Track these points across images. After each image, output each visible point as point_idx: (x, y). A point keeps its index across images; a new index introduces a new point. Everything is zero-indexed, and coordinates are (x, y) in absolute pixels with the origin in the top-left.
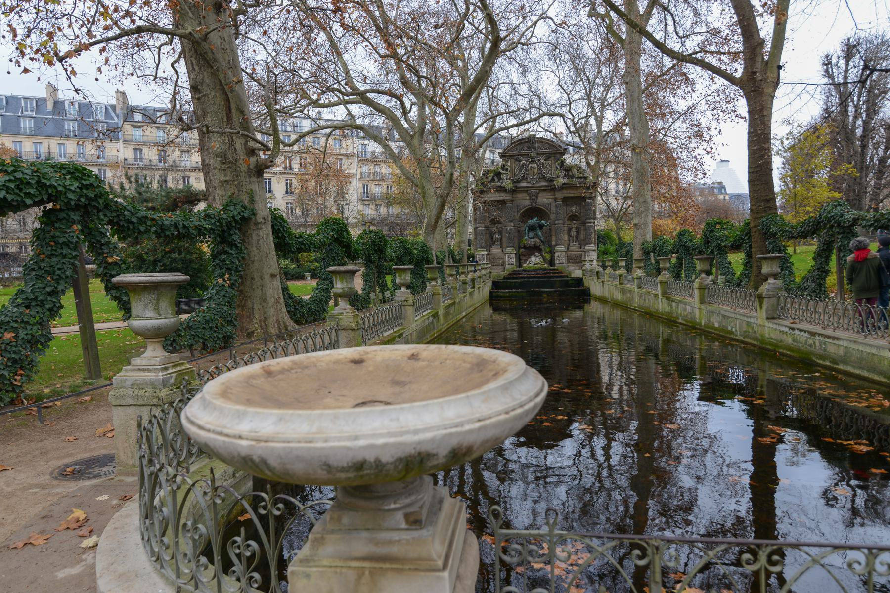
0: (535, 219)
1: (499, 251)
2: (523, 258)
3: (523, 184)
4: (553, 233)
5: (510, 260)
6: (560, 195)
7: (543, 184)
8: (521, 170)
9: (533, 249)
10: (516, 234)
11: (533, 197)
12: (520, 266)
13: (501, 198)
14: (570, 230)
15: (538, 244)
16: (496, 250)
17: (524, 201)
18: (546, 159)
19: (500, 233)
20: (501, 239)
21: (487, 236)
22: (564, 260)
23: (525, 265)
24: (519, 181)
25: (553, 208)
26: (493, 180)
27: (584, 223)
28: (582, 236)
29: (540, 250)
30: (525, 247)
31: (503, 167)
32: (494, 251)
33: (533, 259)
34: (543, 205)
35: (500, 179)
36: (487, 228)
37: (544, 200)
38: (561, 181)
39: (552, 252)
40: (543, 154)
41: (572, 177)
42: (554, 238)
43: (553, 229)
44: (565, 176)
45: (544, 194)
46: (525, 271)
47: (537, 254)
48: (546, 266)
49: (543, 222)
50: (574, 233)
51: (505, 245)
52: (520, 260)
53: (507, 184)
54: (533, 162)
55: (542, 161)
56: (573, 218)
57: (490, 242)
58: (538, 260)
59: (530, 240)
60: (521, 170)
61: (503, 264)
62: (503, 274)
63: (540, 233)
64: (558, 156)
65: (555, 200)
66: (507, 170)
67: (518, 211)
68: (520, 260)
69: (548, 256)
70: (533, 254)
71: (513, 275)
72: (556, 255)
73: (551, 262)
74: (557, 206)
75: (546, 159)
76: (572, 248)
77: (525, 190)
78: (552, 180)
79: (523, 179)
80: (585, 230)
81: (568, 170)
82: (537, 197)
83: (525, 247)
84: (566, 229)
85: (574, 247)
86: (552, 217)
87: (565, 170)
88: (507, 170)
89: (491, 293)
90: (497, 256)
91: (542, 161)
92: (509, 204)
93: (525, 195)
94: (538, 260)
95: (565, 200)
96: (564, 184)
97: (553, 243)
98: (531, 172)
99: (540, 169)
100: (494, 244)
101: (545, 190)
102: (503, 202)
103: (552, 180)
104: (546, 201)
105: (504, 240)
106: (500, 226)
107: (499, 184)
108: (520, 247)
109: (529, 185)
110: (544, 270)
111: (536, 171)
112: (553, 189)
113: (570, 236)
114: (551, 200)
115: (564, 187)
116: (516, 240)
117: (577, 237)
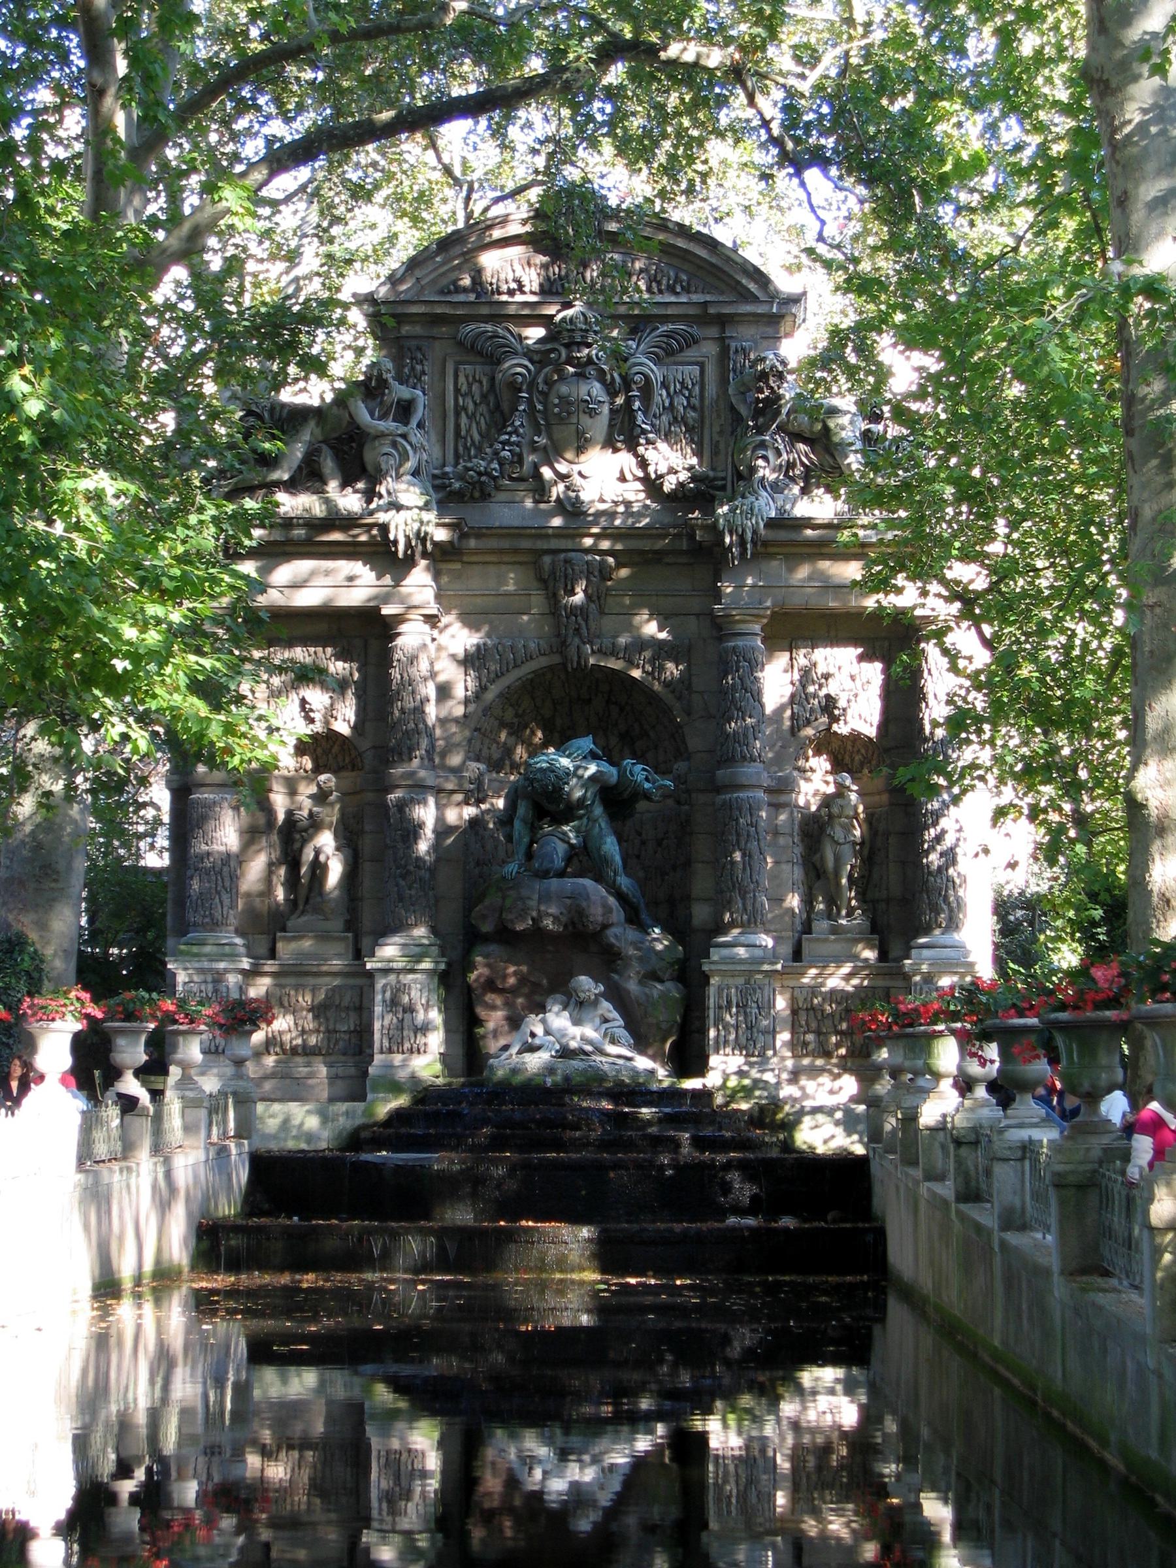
15: (596, 914)
18: (666, 354)
42: (702, 883)
47: (586, 984)
51: (367, 920)
60: (500, 419)
62: (347, 1115)
63: (611, 846)
64: (744, 335)
66: (404, 410)
72: (712, 991)
83: (505, 936)
87: (781, 429)
88: (404, 410)
96: (771, 524)
97: (701, 913)
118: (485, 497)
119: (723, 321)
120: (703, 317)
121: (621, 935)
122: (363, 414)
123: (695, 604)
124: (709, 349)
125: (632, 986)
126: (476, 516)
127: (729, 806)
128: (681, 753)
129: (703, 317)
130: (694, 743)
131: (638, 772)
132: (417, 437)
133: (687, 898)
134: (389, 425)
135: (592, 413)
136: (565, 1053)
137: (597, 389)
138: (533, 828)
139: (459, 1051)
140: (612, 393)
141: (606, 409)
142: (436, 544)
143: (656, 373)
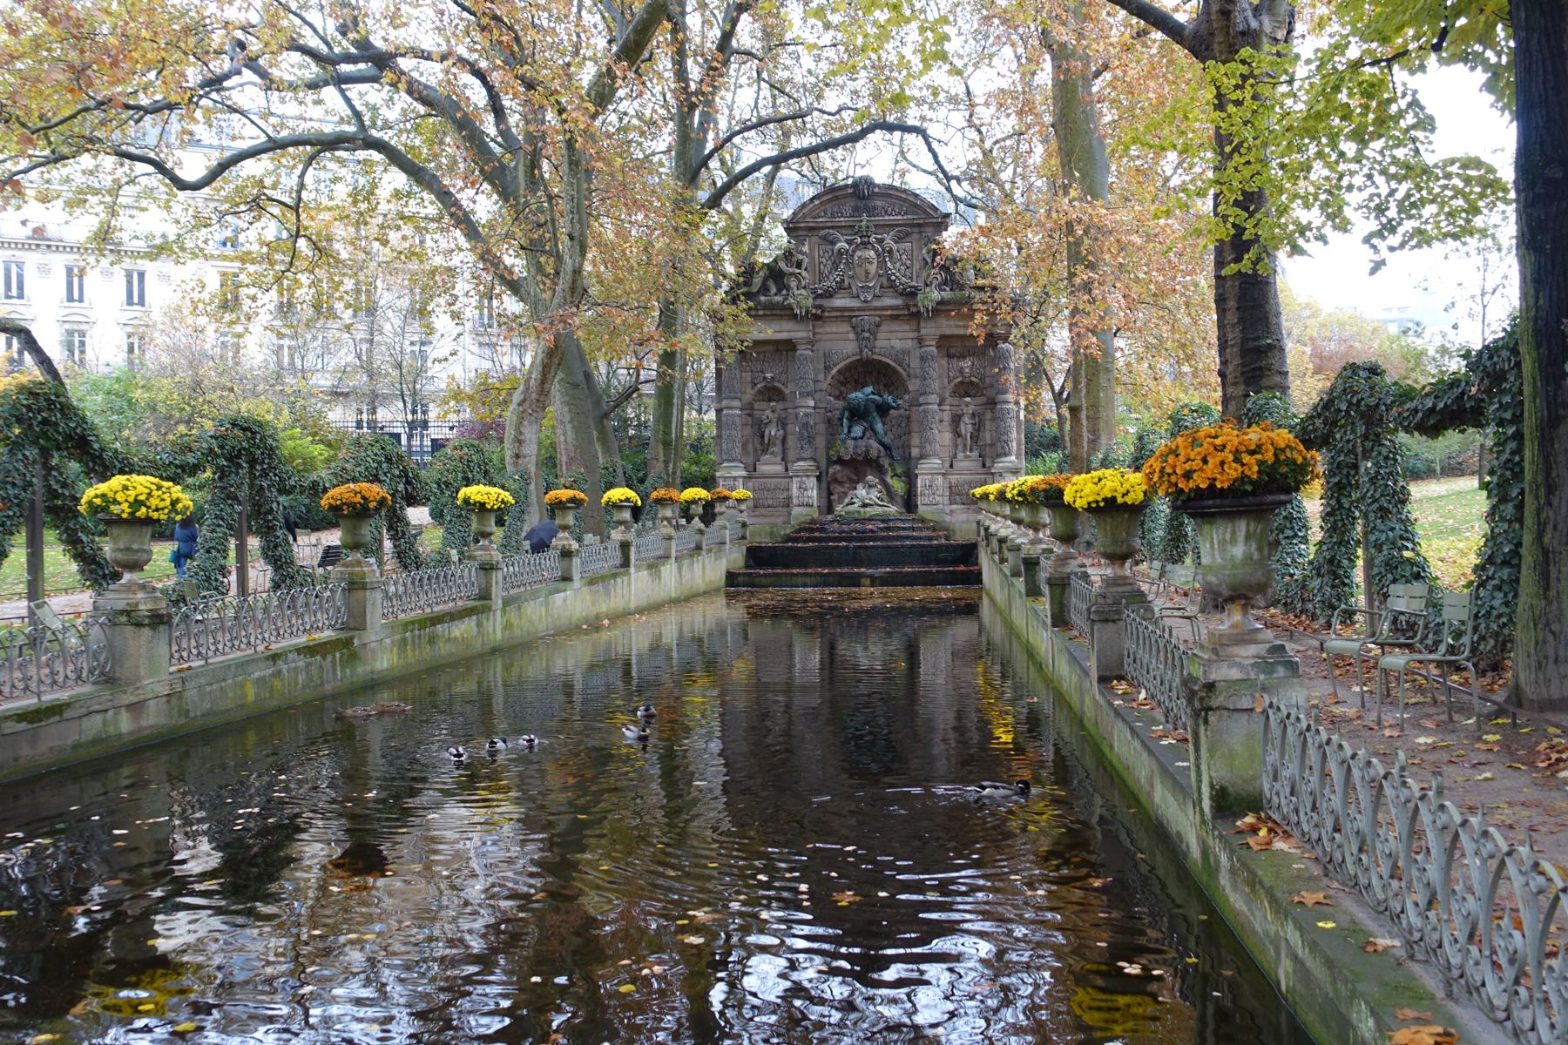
0: (869, 389)
1: (779, 468)
2: (838, 489)
3: (840, 302)
4: (915, 426)
5: (806, 493)
6: (930, 330)
7: (888, 302)
8: (835, 266)
9: (860, 467)
10: (822, 428)
11: (865, 335)
12: (830, 509)
13: (785, 336)
14: (956, 420)
15: (873, 454)
16: (770, 466)
17: (842, 344)
18: (898, 240)
19: (783, 423)
20: (784, 441)
21: (748, 431)
22: (942, 498)
23: (839, 508)
24: (829, 294)
25: (915, 363)
26: (764, 289)
27: (992, 403)
28: (987, 437)
29: (880, 471)
30: (840, 461)
31: (788, 255)
32: (764, 468)
33: (861, 491)
34: (890, 356)
35: (782, 286)
36: (749, 409)
37: (893, 341)
38: (936, 295)
39: (910, 478)
40: (892, 226)
42: (915, 440)
43: (914, 417)
44: (945, 283)
45: (895, 326)
46: (840, 520)
47: (870, 478)
48: (893, 509)
49: (890, 399)
50: (966, 427)
51: (791, 455)
52: (830, 493)
53: (801, 298)
54: (865, 245)
55: (889, 242)
56: (965, 389)
57: (759, 443)
58: (874, 494)
59: (854, 441)
60: (835, 266)
61: (788, 503)
64: (929, 231)
65: (920, 341)
66: (799, 265)
67: (827, 369)
68: (830, 493)
69: (898, 486)
70: (858, 478)
71: (809, 529)
73: (909, 503)
74: (923, 359)
75: (898, 240)
76: (961, 464)
77: (846, 315)
78: (912, 294)
79: (840, 286)
80: (993, 420)
81: (950, 272)
82: (874, 334)
83: (840, 461)
84: (947, 416)
85: (967, 463)
86: (913, 385)
88: (799, 265)
89: (731, 578)
90: (771, 483)
91: (889, 242)
92: (803, 351)
93: (844, 327)
94: (874, 494)
95: (945, 342)
96: (939, 303)
97: (915, 452)
98: (860, 272)
99: (882, 264)
100: (764, 451)
101: (895, 318)
102: (789, 346)
103: (913, 295)
104: (898, 344)
105: (791, 441)
106: (780, 405)
107: (778, 298)
108: (830, 463)
109: (855, 304)
110: (885, 519)
111: (873, 269)
112: (916, 316)
113: (957, 434)
114: (910, 344)
115: (941, 308)
116: (820, 441)
117: (975, 438)
118: (831, 296)
119: (919, 225)
120: (912, 226)
121: (885, 462)
122: (782, 265)
123: (911, 335)
124: (916, 236)
125: (889, 480)
126: (826, 303)
127: (925, 411)
128: (907, 391)
129: (912, 226)
130: (911, 388)
132: (804, 274)
133: (909, 447)
136: (865, 505)
138: (849, 420)
139: (825, 502)
140: (878, 255)
143: (895, 247)
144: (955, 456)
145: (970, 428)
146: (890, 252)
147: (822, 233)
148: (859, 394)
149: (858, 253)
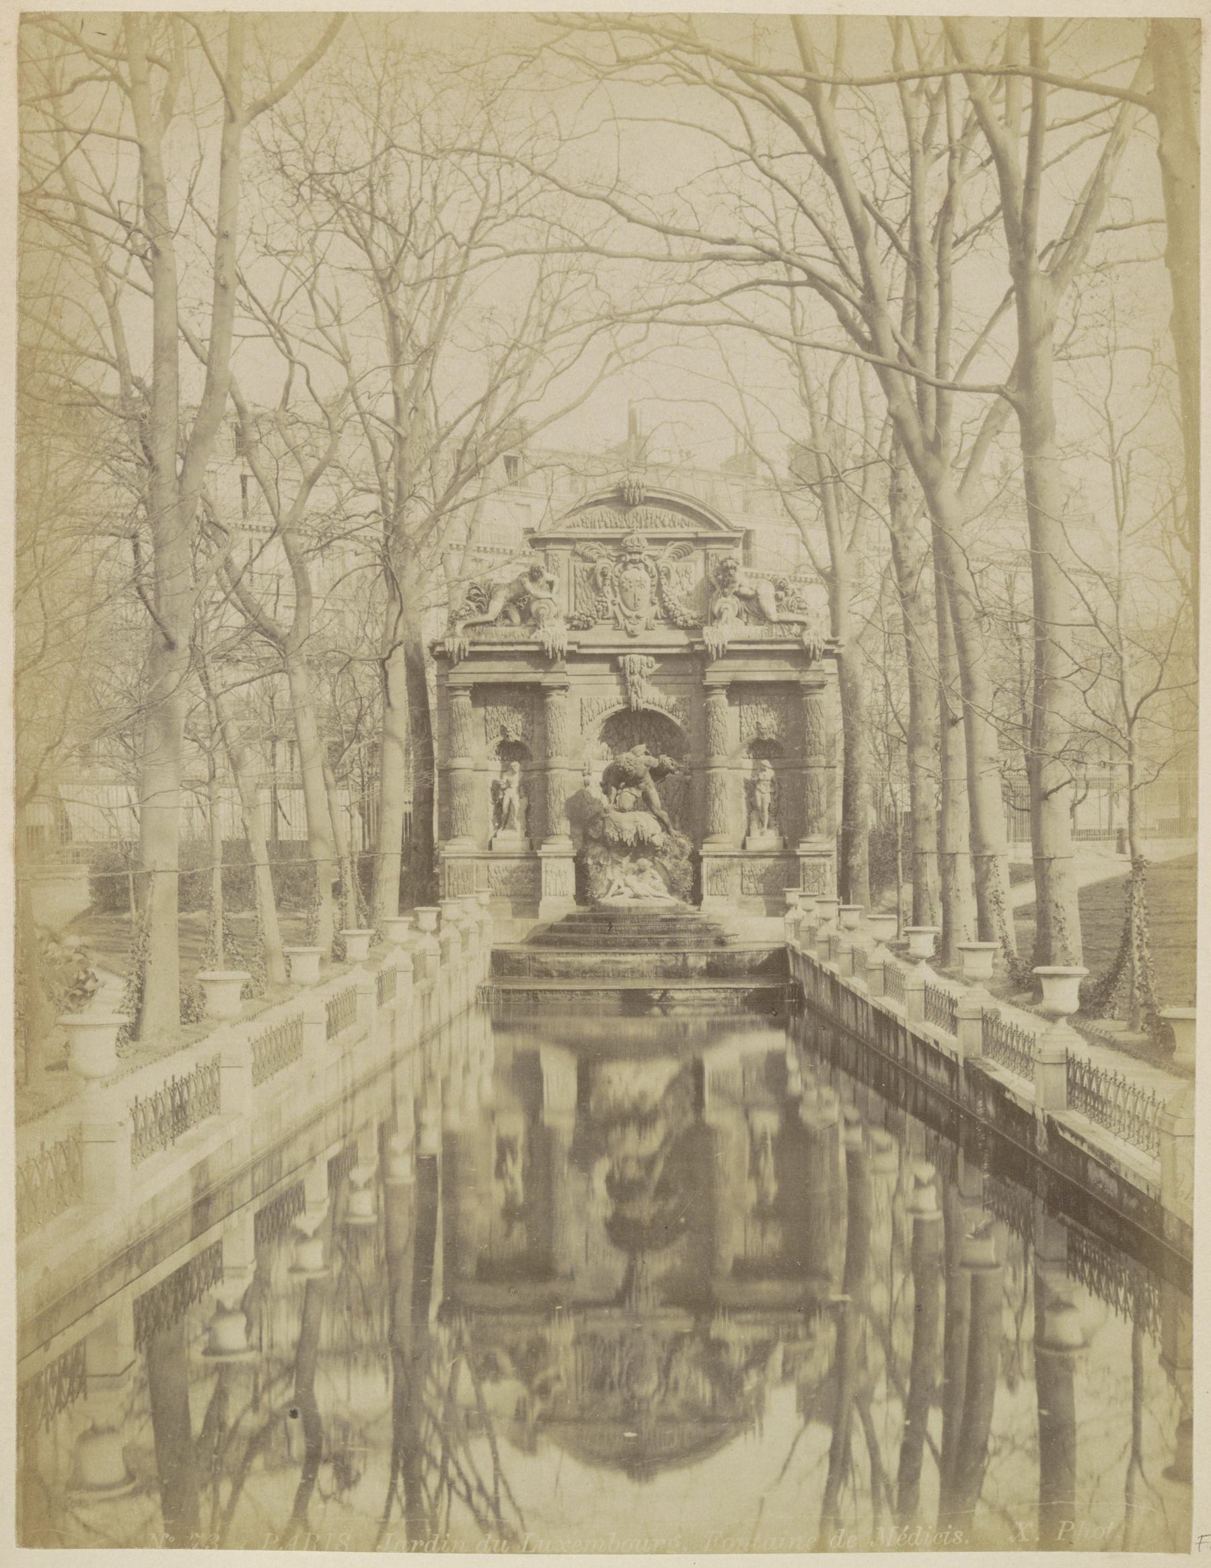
0: (641, 748)
14: (751, 787)
31: (534, 575)
41: (761, 616)
49: (667, 760)
50: (764, 796)
66: (551, 584)
75: (678, 556)
87: (736, 594)
109: (620, 638)
111: (645, 593)
113: (752, 806)
117: (775, 812)
121: (659, 838)
131: (667, 760)
134: (544, 594)
135: (642, 585)
136: (636, 896)
137: (642, 574)
141: (648, 585)
142: (570, 653)
144: (748, 833)
145: (768, 799)
146: (668, 575)
147: (579, 547)
148: (629, 755)
149: (627, 574)
